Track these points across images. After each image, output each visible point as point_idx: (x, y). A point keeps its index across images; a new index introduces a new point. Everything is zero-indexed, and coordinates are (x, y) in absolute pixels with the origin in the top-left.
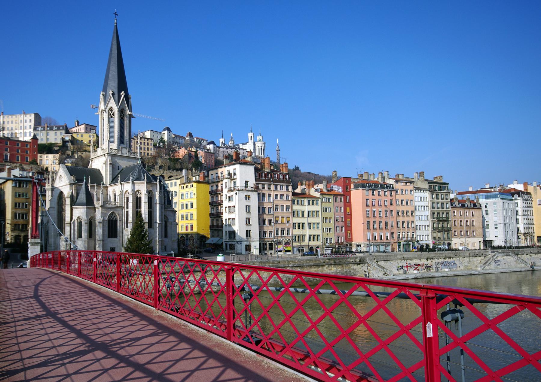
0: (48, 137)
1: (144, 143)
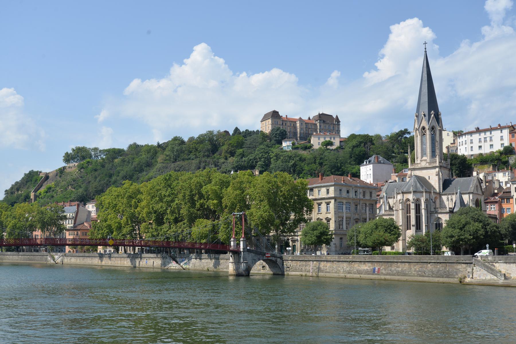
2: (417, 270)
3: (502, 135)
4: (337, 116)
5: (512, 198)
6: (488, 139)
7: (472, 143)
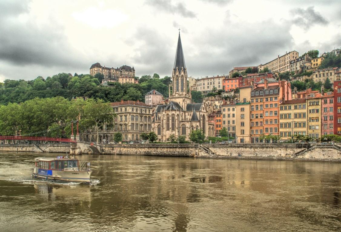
0: (297, 66)
3: (219, 81)
4: (133, 67)
5: (222, 114)
6: (212, 83)
7: (204, 85)
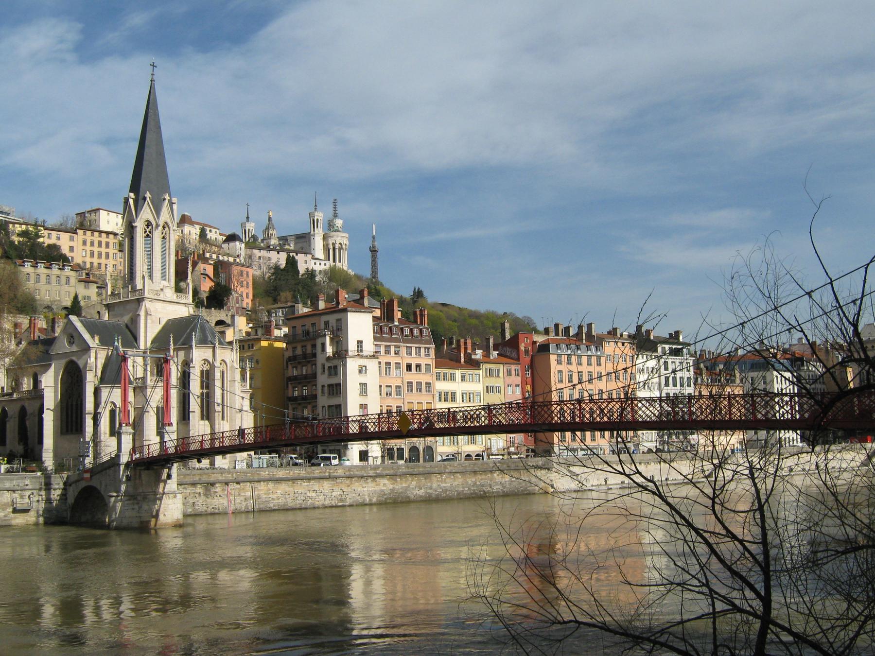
1: (100, 243)
2: (478, 483)
